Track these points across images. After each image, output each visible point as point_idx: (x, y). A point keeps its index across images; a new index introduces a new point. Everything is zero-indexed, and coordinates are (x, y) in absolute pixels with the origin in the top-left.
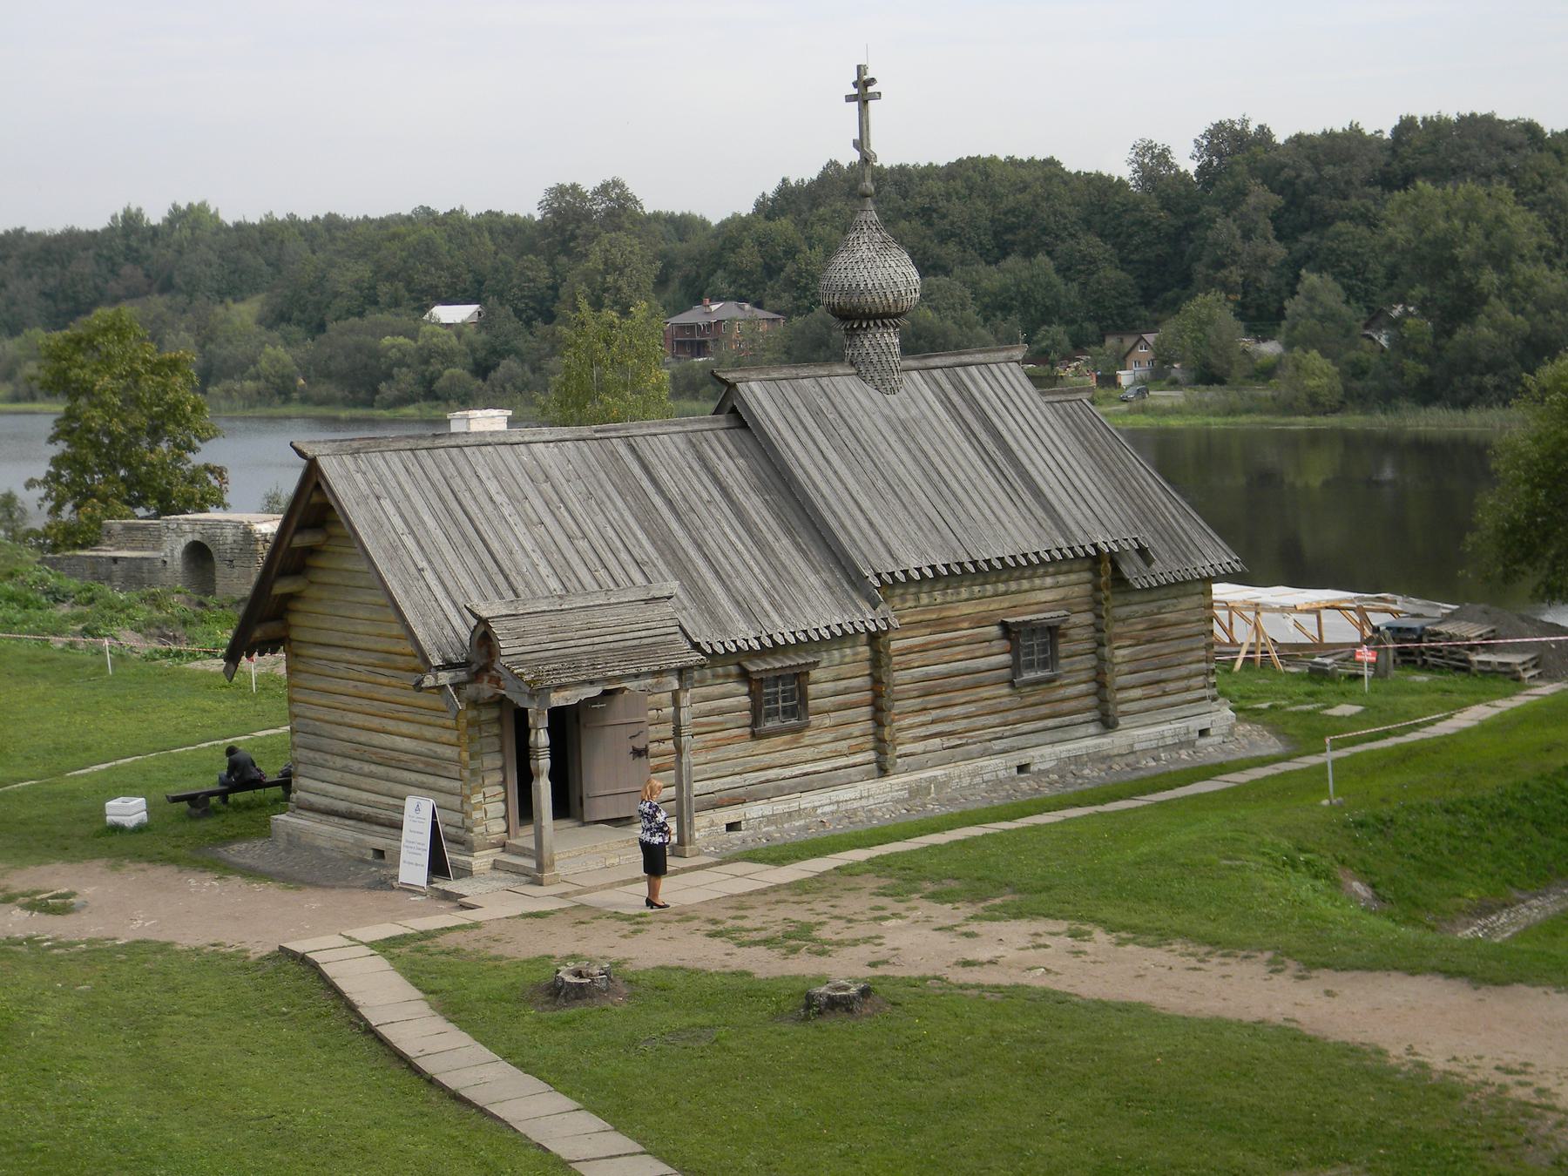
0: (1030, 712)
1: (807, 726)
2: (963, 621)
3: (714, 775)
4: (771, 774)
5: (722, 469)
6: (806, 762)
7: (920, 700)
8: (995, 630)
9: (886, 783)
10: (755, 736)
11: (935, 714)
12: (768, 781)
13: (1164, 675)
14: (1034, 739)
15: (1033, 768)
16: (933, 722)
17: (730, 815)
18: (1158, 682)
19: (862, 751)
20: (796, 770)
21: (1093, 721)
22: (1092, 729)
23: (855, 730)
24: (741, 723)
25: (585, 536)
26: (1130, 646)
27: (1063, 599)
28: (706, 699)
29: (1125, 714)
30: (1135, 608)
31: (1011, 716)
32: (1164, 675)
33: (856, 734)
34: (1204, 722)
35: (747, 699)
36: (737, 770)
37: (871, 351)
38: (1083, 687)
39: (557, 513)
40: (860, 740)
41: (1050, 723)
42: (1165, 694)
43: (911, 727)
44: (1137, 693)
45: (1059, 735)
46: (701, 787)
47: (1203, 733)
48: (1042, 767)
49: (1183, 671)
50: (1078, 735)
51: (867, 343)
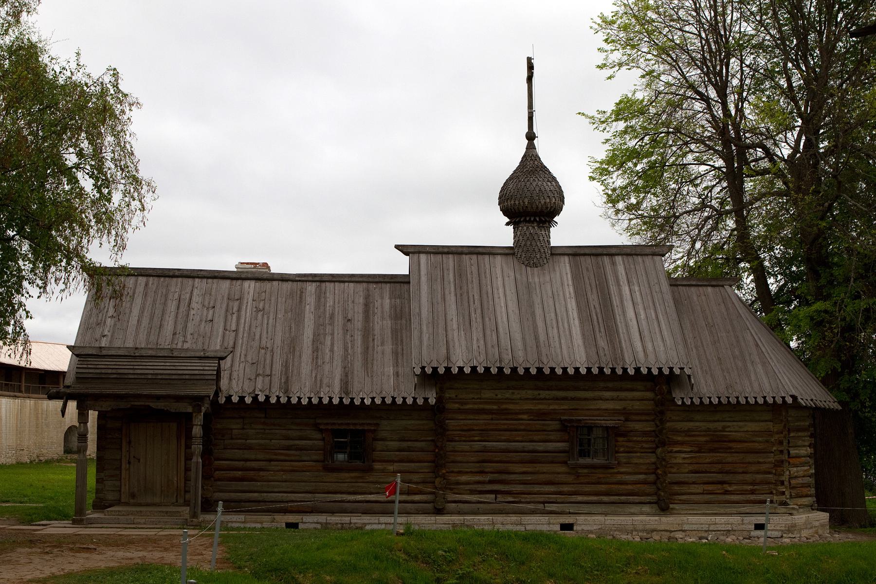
0: (587, 488)
1: (370, 470)
2: (523, 413)
3: (289, 490)
4: (338, 497)
6: (371, 493)
7: (478, 465)
8: (555, 425)
10: (328, 469)
11: (487, 478)
13: (727, 478)
14: (585, 508)
15: (575, 528)
16: (491, 482)
17: (292, 518)
18: (722, 483)
20: (359, 497)
21: (650, 503)
22: (646, 508)
23: (415, 477)
24: (315, 457)
25: (236, 331)
26: (691, 452)
27: (624, 409)
28: (288, 438)
29: (684, 502)
30: (698, 424)
31: (566, 489)
32: (727, 478)
33: (415, 480)
34: (761, 520)
38: (642, 477)
39: (229, 317)
41: (605, 499)
42: (726, 492)
43: (468, 483)
44: (699, 489)
45: (612, 508)
46: (287, 496)
47: (759, 527)
48: (586, 528)
49: (748, 477)
50: (632, 511)
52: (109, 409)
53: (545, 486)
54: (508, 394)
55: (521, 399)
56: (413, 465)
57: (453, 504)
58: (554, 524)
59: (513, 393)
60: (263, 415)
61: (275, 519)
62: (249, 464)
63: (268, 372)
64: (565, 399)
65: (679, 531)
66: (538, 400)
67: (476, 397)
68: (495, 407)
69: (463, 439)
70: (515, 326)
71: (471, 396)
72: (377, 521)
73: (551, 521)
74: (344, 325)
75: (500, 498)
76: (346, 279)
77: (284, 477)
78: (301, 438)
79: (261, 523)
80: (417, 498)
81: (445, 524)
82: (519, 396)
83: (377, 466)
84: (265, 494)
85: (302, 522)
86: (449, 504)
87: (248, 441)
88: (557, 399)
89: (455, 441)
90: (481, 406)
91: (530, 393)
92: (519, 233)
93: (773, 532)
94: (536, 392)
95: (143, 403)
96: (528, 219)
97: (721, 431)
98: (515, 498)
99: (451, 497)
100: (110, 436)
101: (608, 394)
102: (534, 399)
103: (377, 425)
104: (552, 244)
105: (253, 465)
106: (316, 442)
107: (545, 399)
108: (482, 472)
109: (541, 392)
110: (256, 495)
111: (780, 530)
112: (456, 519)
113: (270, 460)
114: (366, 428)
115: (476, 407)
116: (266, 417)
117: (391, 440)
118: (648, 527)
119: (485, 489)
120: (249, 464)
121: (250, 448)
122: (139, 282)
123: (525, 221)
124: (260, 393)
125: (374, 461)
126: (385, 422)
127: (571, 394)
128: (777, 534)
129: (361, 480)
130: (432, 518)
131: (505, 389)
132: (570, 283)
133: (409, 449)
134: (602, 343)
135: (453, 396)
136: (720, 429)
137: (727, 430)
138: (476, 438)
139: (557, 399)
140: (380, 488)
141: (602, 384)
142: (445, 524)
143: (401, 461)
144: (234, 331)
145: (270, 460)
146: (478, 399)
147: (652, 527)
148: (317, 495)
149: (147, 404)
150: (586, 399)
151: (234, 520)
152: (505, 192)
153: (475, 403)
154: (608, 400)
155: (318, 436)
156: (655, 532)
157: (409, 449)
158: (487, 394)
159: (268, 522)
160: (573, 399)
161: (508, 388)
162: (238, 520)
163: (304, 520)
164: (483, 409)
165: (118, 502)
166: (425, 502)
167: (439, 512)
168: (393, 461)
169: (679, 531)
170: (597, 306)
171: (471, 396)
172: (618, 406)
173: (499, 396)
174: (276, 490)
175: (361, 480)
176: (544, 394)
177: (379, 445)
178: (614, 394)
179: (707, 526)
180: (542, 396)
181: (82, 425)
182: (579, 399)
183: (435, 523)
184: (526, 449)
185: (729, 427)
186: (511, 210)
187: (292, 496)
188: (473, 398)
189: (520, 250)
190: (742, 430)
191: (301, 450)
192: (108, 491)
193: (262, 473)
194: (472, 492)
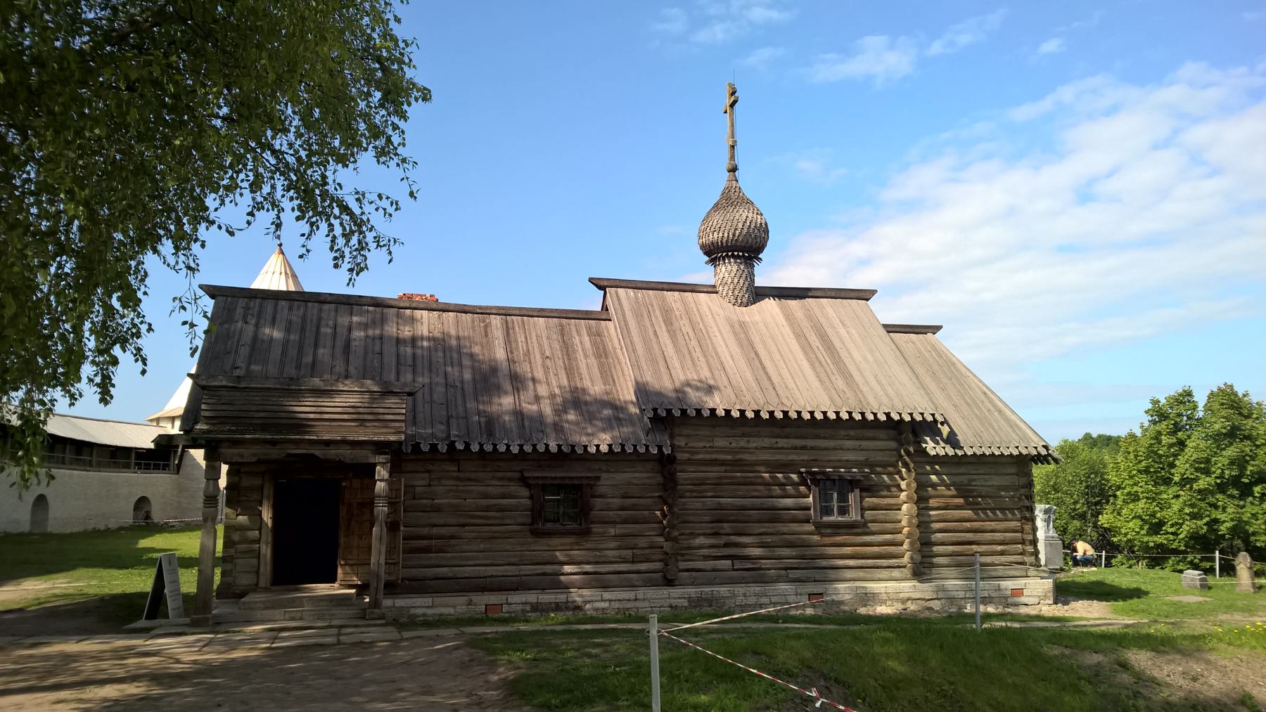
3: (488, 562)
5: (576, 340)
9: (664, 592)
10: (537, 534)
12: (544, 574)
19: (648, 561)
24: (520, 520)
28: (486, 496)
33: (641, 545)
35: (527, 502)
36: (513, 560)
37: (726, 275)
40: (647, 551)
43: (701, 547)
50: (881, 576)
51: (723, 269)
52: (254, 459)
53: (785, 549)
54: (743, 443)
55: (756, 448)
56: (637, 526)
57: (686, 573)
58: (801, 595)
59: (748, 441)
60: (455, 468)
61: (471, 601)
62: (435, 530)
63: (462, 414)
64: (804, 448)
65: (935, 599)
66: (775, 449)
67: (708, 445)
68: (729, 457)
69: (695, 494)
70: (742, 364)
71: (702, 444)
72: (599, 598)
73: (799, 591)
74: (543, 362)
75: (738, 565)
76: (535, 314)
77: (482, 546)
78: (503, 496)
79: (454, 607)
80: (643, 567)
81: (680, 598)
82: (754, 445)
83: (597, 528)
84: (457, 569)
85: (507, 603)
86: (680, 574)
87: (436, 501)
88: (796, 448)
89: (686, 497)
90: (714, 456)
91: (767, 442)
92: (718, 271)
93: (1030, 599)
94: (774, 440)
95: (305, 451)
96: (730, 254)
97: (966, 485)
98: (754, 563)
99: (682, 565)
100: (245, 498)
101: (849, 444)
102: (770, 448)
103: (598, 478)
104: (756, 285)
105: (442, 531)
106: (522, 501)
107: (782, 448)
108: (716, 534)
109: (779, 440)
110: (445, 569)
111: (1039, 597)
112: (692, 591)
113: (464, 525)
114: (584, 482)
115: (708, 457)
116: (459, 471)
117: (612, 497)
118: (901, 596)
119: (720, 554)
120: (435, 530)
121: (438, 509)
122: (279, 307)
123: (733, 256)
124: (456, 439)
125: (592, 523)
126: (604, 475)
127: (810, 443)
128: (1036, 600)
129: (577, 547)
130: (665, 592)
131: (739, 436)
132: (784, 323)
133: (633, 508)
134: (840, 383)
135: (683, 444)
136: (966, 482)
137: (974, 483)
138: (709, 494)
139: (796, 448)
140: (600, 556)
141: (843, 432)
142: (680, 598)
143: (625, 522)
144: (411, 366)
145: (464, 525)
146: (710, 447)
147: (907, 595)
148: (522, 567)
149: (312, 452)
150: (826, 449)
151: (418, 604)
152: (711, 223)
153: (708, 453)
154: (849, 450)
155: (525, 492)
156: (910, 602)
157: (633, 508)
158: (721, 443)
159: (462, 605)
160: (812, 448)
161: (743, 435)
162: (423, 604)
163: (509, 600)
164: (716, 460)
165: (255, 588)
166: (654, 572)
167: (669, 582)
168: (614, 523)
169: (935, 599)
170: (821, 348)
171: (702, 444)
172: (860, 457)
173: (734, 445)
174: (471, 563)
175: (577, 547)
176: (782, 442)
177: (598, 503)
178: (857, 443)
179: (963, 593)
180: (780, 445)
181: (211, 482)
182: (820, 449)
183: (669, 598)
184: (765, 506)
185: (975, 480)
186: (717, 243)
187: (491, 570)
188: (705, 447)
189: (726, 288)
190: (988, 484)
191: (503, 510)
192: (240, 572)
193: (453, 542)
194: (706, 558)
